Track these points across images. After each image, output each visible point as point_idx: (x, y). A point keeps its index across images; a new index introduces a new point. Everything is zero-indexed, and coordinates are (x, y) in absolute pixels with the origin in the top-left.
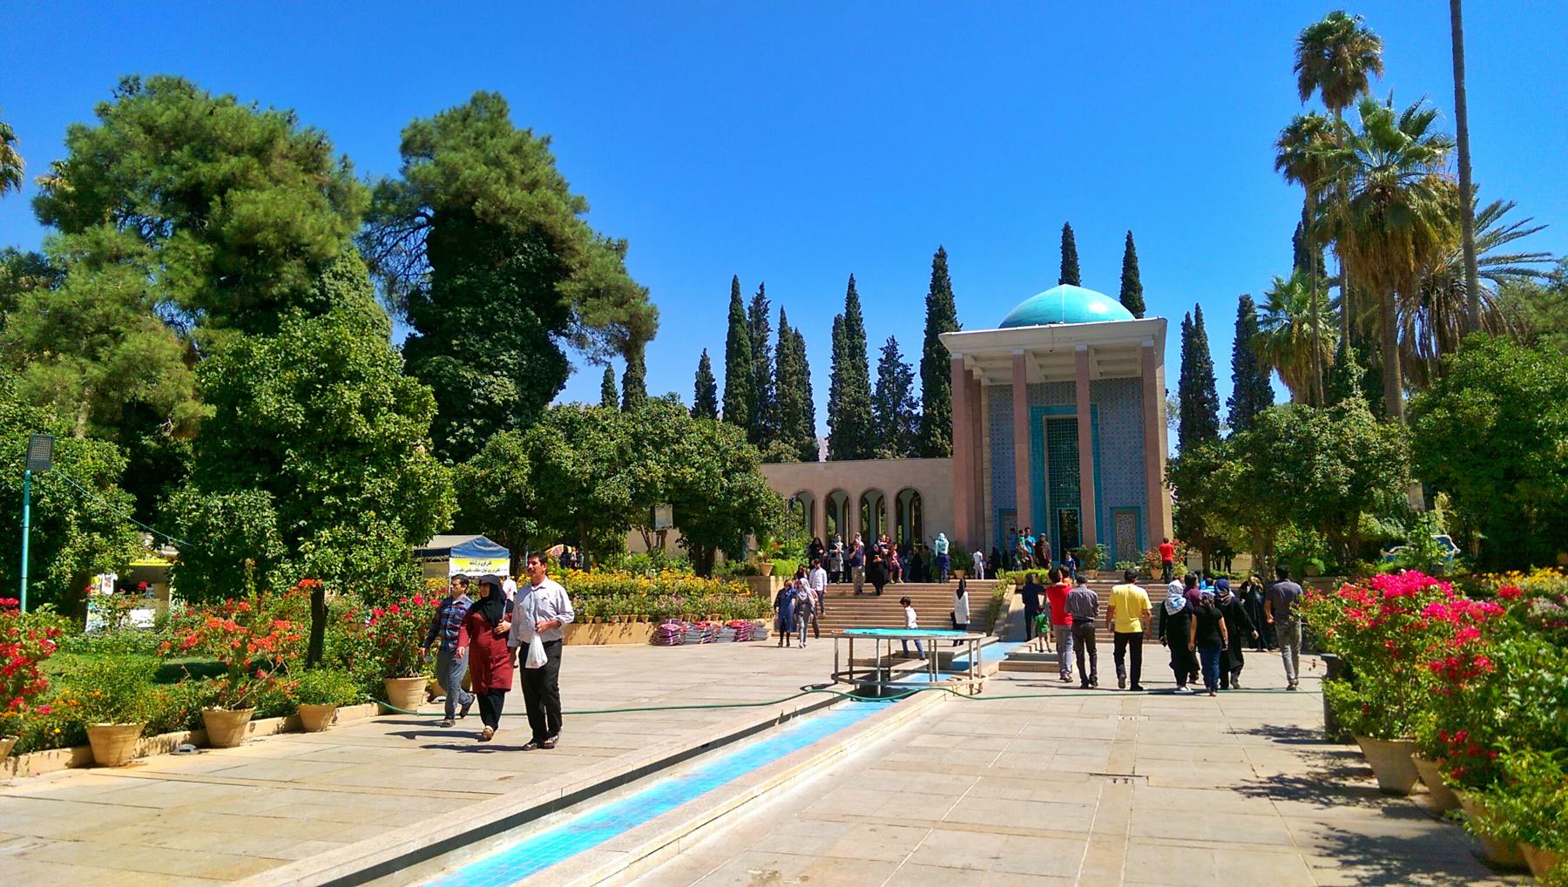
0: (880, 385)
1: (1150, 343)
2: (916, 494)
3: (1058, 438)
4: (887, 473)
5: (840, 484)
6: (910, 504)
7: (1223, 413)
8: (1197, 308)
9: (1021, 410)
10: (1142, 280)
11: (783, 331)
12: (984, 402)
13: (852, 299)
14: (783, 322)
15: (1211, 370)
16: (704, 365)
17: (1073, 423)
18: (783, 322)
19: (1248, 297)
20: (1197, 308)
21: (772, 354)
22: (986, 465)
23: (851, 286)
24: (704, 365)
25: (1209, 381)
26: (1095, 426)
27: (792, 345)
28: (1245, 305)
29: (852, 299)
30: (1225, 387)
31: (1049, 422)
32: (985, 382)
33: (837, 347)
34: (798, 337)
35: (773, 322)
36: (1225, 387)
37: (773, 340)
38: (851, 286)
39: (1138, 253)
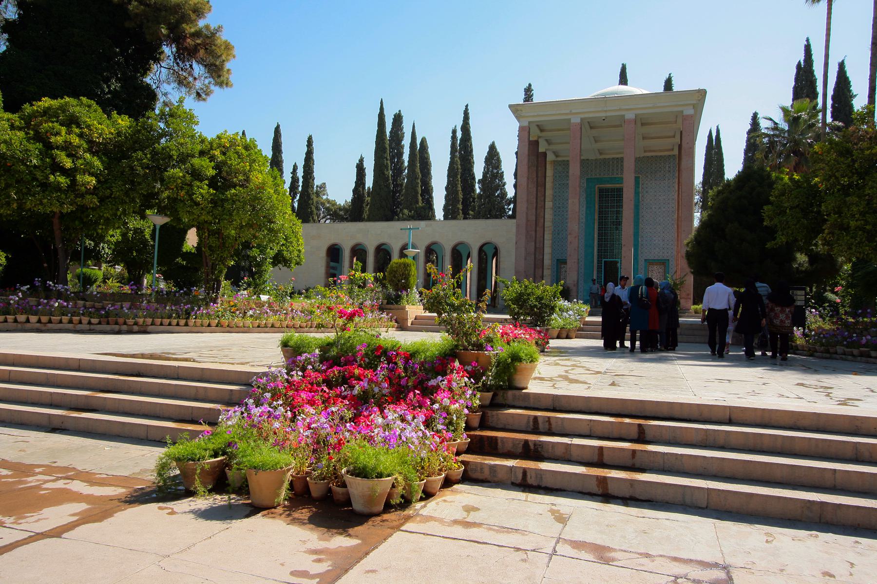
1: (689, 111)
2: (496, 248)
3: (607, 202)
4: (473, 232)
5: (436, 239)
6: (487, 254)
9: (575, 170)
12: (549, 172)
16: (361, 160)
17: (620, 191)
22: (547, 224)
24: (361, 160)
26: (637, 193)
28: (755, 117)
32: (550, 157)
37: (406, 142)
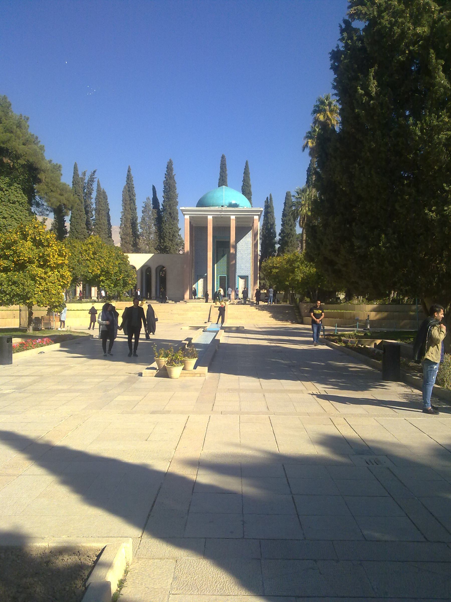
0: (143, 219)
7: (278, 238)
8: (270, 195)
10: (251, 182)
11: (99, 190)
13: (129, 178)
14: (99, 185)
15: (274, 222)
18: (99, 185)
19: (289, 192)
20: (270, 195)
21: (93, 201)
23: (129, 171)
25: (273, 225)
27: (102, 197)
28: (288, 195)
29: (129, 178)
30: (278, 229)
31: (217, 242)
33: (124, 200)
34: (104, 192)
35: (95, 186)
36: (278, 229)
38: (129, 171)
39: (250, 171)
